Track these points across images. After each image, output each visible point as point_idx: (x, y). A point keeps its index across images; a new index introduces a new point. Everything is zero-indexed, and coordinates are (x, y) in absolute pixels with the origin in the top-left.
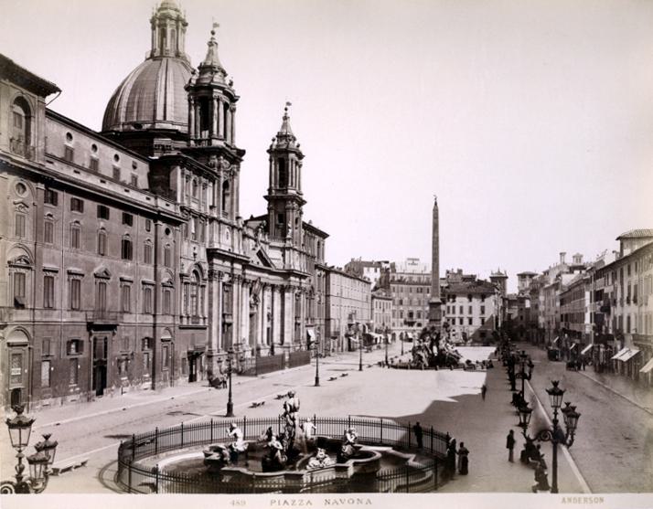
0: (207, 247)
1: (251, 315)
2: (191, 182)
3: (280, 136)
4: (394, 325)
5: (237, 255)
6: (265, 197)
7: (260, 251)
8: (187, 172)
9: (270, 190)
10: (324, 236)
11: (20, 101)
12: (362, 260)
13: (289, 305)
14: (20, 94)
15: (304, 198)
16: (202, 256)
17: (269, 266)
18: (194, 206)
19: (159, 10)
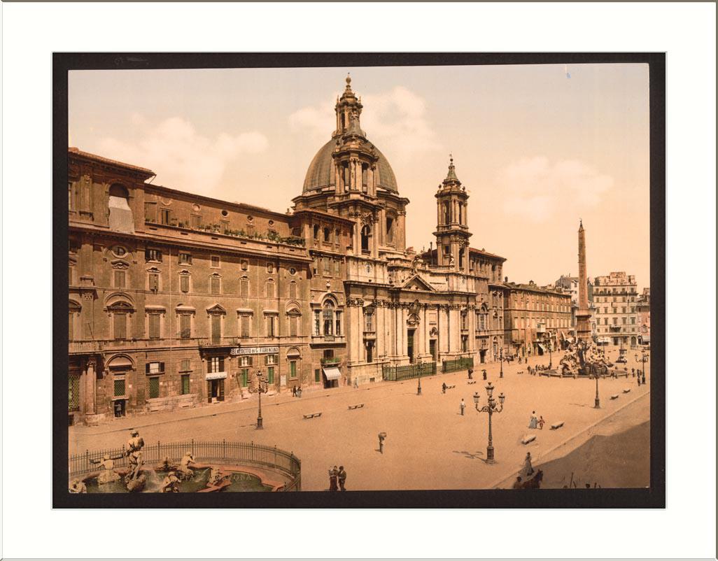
3: (445, 183)
4: (598, 330)
6: (434, 234)
9: (438, 227)
12: (571, 276)
13: (488, 319)
15: (470, 231)
17: (429, 290)
19: (341, 99)
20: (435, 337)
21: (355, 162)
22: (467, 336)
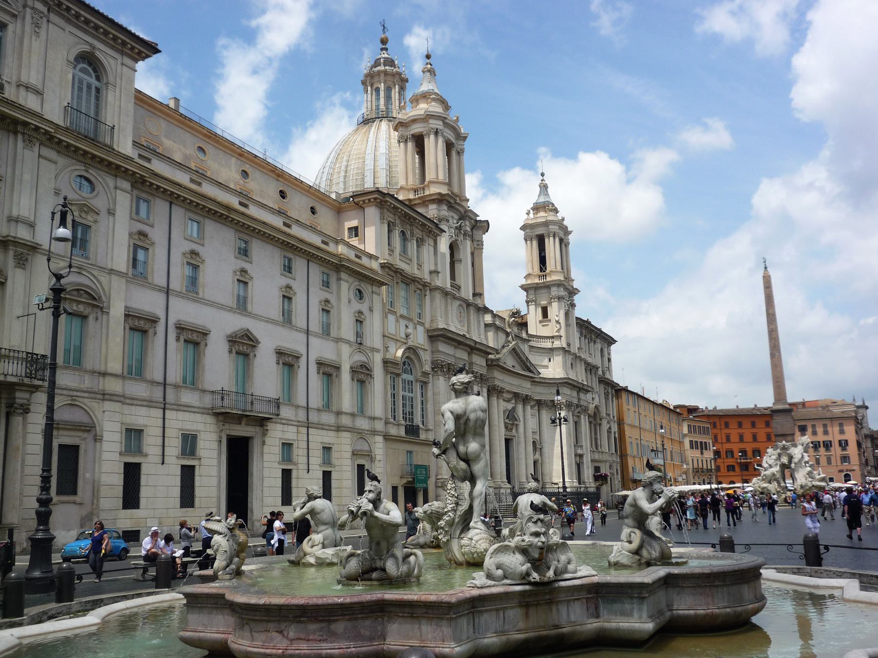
0: (427, 325)
1: (508, 441)
2: (396, 234)
3: (537, 208)
5: (476, 342)
6: (522, 287)
7: (514, 349)
8: (390, 217)
10: (610, 341)
11: (88, 59)
14: (86, 48)
15: (576, 285)
16: (420, 338)
17: (531, 371)
18: (402, 266)
20: (537, 456)
21: (436, 133)
22: (581, 456)
